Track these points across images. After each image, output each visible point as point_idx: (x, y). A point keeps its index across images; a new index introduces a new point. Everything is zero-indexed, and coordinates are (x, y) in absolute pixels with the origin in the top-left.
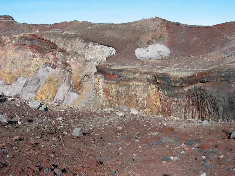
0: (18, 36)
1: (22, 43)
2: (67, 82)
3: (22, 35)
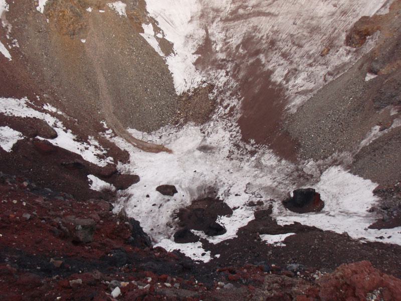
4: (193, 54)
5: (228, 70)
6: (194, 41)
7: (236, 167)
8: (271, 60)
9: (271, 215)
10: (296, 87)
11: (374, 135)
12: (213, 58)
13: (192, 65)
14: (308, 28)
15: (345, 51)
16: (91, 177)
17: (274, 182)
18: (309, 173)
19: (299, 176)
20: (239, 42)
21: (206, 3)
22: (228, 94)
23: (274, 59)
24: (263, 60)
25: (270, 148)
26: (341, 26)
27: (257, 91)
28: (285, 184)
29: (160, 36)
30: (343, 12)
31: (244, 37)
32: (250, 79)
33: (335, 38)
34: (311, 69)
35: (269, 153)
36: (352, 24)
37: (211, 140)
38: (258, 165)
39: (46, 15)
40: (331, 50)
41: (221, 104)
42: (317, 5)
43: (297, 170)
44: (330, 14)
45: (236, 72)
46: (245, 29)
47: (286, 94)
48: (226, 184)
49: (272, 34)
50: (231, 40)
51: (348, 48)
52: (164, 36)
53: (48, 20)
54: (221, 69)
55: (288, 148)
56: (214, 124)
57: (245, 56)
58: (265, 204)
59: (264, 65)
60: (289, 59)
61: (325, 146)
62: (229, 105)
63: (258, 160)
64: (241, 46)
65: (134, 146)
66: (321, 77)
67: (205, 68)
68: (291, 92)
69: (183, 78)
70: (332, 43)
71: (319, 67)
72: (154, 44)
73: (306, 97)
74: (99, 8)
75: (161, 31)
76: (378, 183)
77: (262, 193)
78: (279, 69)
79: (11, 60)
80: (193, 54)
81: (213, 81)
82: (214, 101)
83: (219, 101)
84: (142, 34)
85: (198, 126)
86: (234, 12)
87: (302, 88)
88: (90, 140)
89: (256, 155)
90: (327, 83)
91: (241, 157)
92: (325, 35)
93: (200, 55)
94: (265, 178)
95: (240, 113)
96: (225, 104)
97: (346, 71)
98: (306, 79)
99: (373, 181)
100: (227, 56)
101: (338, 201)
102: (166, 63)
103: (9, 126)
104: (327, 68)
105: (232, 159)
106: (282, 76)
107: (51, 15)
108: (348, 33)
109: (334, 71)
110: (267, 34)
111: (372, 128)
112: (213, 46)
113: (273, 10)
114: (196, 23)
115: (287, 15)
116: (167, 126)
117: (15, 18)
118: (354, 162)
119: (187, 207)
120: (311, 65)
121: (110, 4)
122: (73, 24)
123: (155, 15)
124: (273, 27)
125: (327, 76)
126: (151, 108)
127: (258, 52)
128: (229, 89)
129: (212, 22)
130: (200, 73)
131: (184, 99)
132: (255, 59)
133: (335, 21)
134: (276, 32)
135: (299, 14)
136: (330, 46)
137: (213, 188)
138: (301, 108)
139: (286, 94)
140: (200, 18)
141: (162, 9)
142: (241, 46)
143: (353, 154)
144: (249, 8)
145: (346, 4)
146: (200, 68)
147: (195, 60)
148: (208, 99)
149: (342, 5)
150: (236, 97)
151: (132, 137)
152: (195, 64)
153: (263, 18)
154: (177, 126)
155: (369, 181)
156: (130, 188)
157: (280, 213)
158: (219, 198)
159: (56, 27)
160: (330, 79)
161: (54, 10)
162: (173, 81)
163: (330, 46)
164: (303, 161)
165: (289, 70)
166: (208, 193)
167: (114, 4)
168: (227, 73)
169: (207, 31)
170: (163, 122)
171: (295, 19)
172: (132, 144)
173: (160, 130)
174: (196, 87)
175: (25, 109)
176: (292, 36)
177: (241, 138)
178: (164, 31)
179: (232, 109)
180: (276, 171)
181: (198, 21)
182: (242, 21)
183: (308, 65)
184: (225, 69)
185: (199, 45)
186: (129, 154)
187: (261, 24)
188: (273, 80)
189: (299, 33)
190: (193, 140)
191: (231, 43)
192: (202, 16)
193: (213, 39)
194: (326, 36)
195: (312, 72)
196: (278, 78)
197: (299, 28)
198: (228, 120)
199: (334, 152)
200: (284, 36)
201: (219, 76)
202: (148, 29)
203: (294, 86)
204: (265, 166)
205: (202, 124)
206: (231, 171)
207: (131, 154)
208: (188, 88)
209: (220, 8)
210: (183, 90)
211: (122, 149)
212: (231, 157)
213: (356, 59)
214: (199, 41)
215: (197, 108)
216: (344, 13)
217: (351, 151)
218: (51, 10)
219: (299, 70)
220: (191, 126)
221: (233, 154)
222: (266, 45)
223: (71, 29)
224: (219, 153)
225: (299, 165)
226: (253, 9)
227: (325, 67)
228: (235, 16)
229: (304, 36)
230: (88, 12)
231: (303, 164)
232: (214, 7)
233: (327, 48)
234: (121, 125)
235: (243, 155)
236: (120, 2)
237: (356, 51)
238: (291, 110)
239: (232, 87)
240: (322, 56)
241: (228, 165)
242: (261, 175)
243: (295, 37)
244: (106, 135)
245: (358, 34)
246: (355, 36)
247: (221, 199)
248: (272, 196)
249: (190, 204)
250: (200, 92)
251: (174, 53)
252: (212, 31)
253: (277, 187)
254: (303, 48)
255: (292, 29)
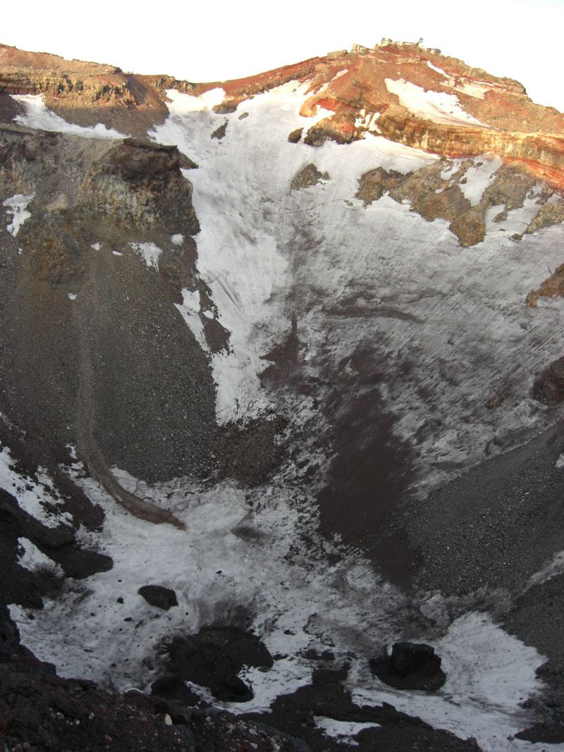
0: (523, 136)
1: (529, 157)
2: (416, 156)
3: (535, 135)
4: (262, 358)
5: (319, 399)
6: (268, 337)
7: (298, 579)
8: (398, 396)
9: (343, 683)
10: (434, 454)
11: (556, 567)
12: (295, 373)
13: (255, 377)
14: (472, 354)
15: (530, 408)
16: (24, 542)
17: (363, 621)
18: (429, 616)
19: (411, 619)
20: (349, 353)
21: (302, 275)
22: (310, 441)
23: (404, 396)
24: (385, 395)
25: (366, 556)
26: (529, 363)
27: (362, 447)
28: (381, 629)
29: (209, 314)
30: (535, 339)
31: (357, 347)
32: (355, 424)
33: (517, 382)
34: (465, 427)
35: (363, 565)
36: (547, 364)
37: (264, 520)
38: (339, 584)
39: (20, 241)
40: (505, 401)
41: (294, 458)
42: (494, 320)
43: (409, 606)
44: (512, 338)
45: (332, 405)
46: (362, 334)
47: (414, 462)
48: (272, 608)
49: (408, 351)
50: (334, 347)
51: (535, 403)
52: (216, 316)
53: (20, 250)
54: (307, 394)
55: (400, 563)
56: (273, 491)
57: (353, 380)
58: (337, 659)
59: (384, 404)
60: (430, 401)
61: (468, 571)
62: (307, 461)
63: (341, 575)
64: (350, 361)
65: (118, 502)
66: (481, 444)
67: (278, 387)
68: (424, 460)
69: (234, 396)
70: (509, 389)
71: (481, 427)
72: (196, 326)
73: (448, 475)
74: (114, 247)
75: (213, 308)
76: (549, 656)
77: (336, 638)
78: (410, 415)
80: (262, 358)
81: (288, 414)
82: (282, 450)
83: (291, 451)
84: (178, 306)
85: (243, 488)
86: (348, 301)
87: (444, 458)
88: (40, 473)
89: (338, 565)
90: (489, 457)
91: (311, 562)
92: (499, 372)
93: (273, 363)
94: (347, 610)
95: (325, 481)
96: (301, 459)
97: (526, 443)
98: (455, 443)
99: (540, 652)
100: (321, 374)
101: (471, 677)
102: (210, 365)
104: (495, 431)
105: (293, 563)
106: (413, 430)
107: (28, 242)
108: (539, 377)
109: (506, 438)
110: (400, 351)
111: (555, 553)
112: (301, 353)
113: (417, 312)
114: (277, 306)
115: (440, 325)
116: (186, 477)
118: (513, 611)
119: (189, 636)
120: (466, 420)
121: (134, 244)
122: (62, 264)
123: (209, 279)
124: (412, 340)
125: (491, 445)
126: (165, 439)
127: (378, 378)
128: (313, 434)
129: (308, 310)
130: (268, 395)
131: (227, 434)
132: (370, 389)
133: (520, 352)
134: (417, 350)
135: (461, 328)
136: (505, 393)
137: (246, 610)
138: (436, 493)
139: (414, 462)
140: (287, 299)
141: (223, 270)
142: (350, 361)
143: (515, 594)
144: (376, 299)
145: (543, 327)
146: (269, 384)
147: (262, 369)
148: (273, 444)
149: (536, 328)
150: (324, 450)
151: (117, 485)
152: (261, 376)
153: (399, 322)
154: (204, 480)
155: (532, 651)
156: (90, 578)
157: (361, 683)
158: (253, 631)
159: (31, 264)
160: (496, 451)
161: (36, 235)
162: (215, 398)
163: (505, 393)
164: (422, 592)
165: (426, 421)
166: (234, 617)
167: (142, 246)
168: (316, 404)
169: (294, 324)
170: (180, 469)
171: (453, 336)
172: (113, 496)
173: (171, 483)
174: (255, 418)
176: (442, 362)
177: (317, 526)
178: (219, 308)
179: (312, 470)
180: (369, 601)
181: (283, 303)
182: (361, 318)
183: (461, 418)
184: (313, 396)
185: (275, 345)
186: (104, 515)
187: (393, 330)
188: (395, 433)
189: (455, 359)
190: (229, 514)
191: (332, 353)
192: (291, 297)
193: (302, 339)
194: (500, 375)
195: (467, 432)
196: (405, 430)
197: (456, 352)
198: (301, 488)
199: (481, 585)
200: (429, 360)
201: (301, 406)
202: (191, 300)
203: (430, 451)
204: (352, 589)
205: (251, 487)
206: (287, 584)
207: (109, 515)
208: (239, 416)
209: (326, 290)
210: (230, 418)
211: (94, 503)
212: (293, 559)
213: (546, 425)
214: (277, 337)
215: (245, 457)
216: (537, 342)
217: (510, 590)
218: (31, 234)
219: (444, 425)
220: (231, 486)
221: (298, 554)
222: (395, 369)
223: (57, 272)
224: (271, 547)
225: (414, 597)
226: (383, 303)
227: (491, 428)
228: (348, 308)
229: (464, 366)
230: (94, 249)
231: (422, 597)
232: (315, 285)
233: (499, 395)
234: (102, 458)
235: (314, 559)
236: (153, 244)
237: (547, 412)
238: (418, 494)
239: (320, 431)
240: (489, 408)
241: (284, 572)
242: (340, 603)
243: (448, 365)
244: (70, 472)
245: (554, 383)
246: (550, 385)
247: (256, 634)
248: (353, 647)
249: (197, 632)
250: (260, 429)
251: (227, 349)
252: (304, 325)
253: (365, 630)
254: (457, 388)
255: (444, 351)
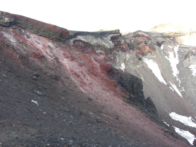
79: (182, 97)
103: (189, 131)
117: (182, 77)
175: (192, 122)
